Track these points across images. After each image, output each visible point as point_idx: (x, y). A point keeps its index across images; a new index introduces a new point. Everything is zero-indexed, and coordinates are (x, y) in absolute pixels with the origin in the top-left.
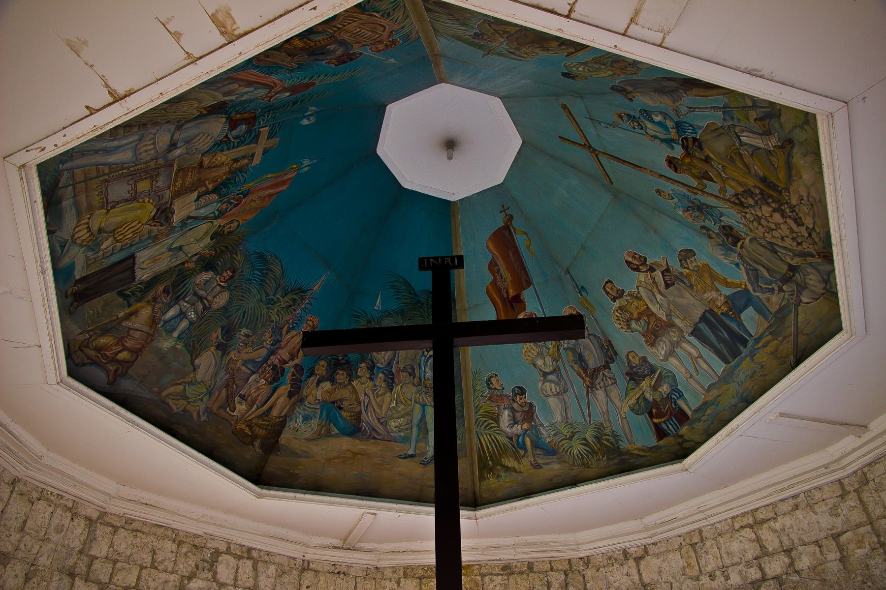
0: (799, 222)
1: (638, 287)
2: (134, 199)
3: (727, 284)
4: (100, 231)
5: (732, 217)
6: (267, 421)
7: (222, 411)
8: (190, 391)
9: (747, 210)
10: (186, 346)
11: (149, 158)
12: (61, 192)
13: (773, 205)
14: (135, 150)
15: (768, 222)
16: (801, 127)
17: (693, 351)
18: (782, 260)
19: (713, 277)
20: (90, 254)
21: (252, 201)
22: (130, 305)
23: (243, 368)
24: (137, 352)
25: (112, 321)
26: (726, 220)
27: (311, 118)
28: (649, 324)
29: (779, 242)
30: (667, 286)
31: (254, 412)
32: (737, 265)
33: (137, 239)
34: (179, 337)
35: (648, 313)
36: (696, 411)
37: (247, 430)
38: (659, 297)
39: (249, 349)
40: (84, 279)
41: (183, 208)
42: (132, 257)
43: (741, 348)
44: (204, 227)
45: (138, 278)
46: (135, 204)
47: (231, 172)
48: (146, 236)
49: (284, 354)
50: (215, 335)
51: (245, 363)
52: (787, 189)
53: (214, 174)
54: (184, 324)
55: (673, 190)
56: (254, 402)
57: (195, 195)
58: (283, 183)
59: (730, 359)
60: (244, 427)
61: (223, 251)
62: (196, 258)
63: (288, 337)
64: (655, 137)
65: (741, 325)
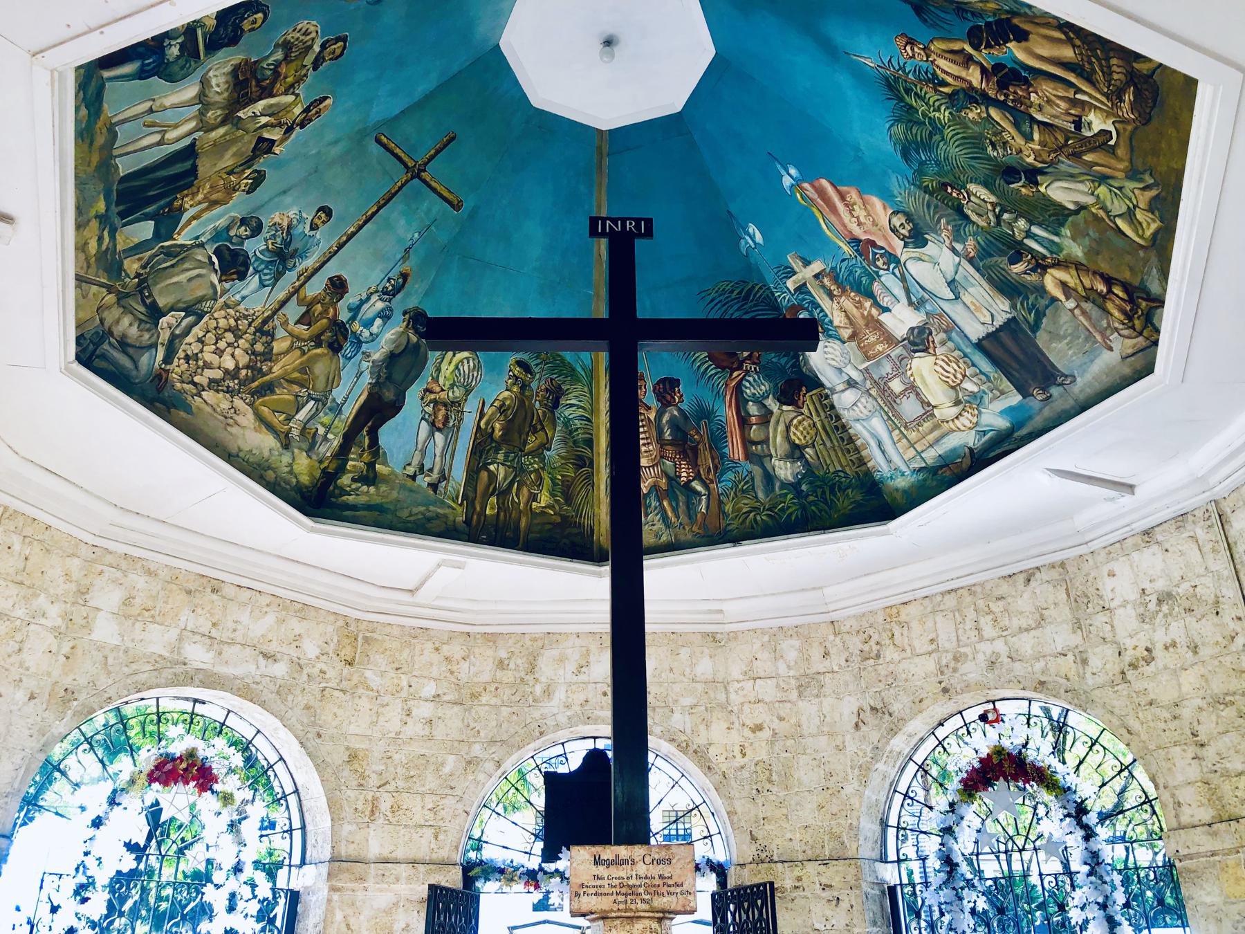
0: (214, 384)
1: (297, 95)
2: (912, 388)
3: (194, 218)
4: (957, 403)
5: (252, 295)
6: (1090, 63)
7: (1120, 152)
8: (1118, 207)
9: (252, 330)
10: (1062, 225)
11: (870, 399)
12: (930, 462)
13: (244, 372)
14: (867, 419)
15: (229, 345)
16: (290, 465)
17: (171, 135)
18: (172, 309)
19: (214, 204)
20: (986, 399)
21: (860, 224)
22: (1054, 300)
23: (1036, 136)
24: (1109, 281)
25: (1084, 313)
26: (254, 282)
27: (751, 231)
28: (258, 82)
29: (197, 331)
30: (261, 140)
31: (1090, 96)
32: (197, 238)
33: (957, 353)
34: (1057, 234)
35: (268, 92)
36: (101, 89)
37: (1129, 97)
38: (264, 120)
39: (1006, 137)
40: (1023, 390)
41: (901, 320)
42: (979, 345)
43: (121, 208)
44: (914, 268)
45: (1009, 316)
46: (919, 383)
47: (844, 291)
48: (950, 344)
49: (974, 76)
50: (1023, 190)
51: (1029, 138)
52: (251, 405)
53: (855, 310)
54: (1036, 230)
55: (318, 245)
56: (1074, 102)
57: (884, 318)
58: (822, 193)
59: (121, 187)
60: (1126, 106)
61: (936, 207)
62: (959, 247)
63: (949, 80)
64: (368, 298)
65: (147, 217)
